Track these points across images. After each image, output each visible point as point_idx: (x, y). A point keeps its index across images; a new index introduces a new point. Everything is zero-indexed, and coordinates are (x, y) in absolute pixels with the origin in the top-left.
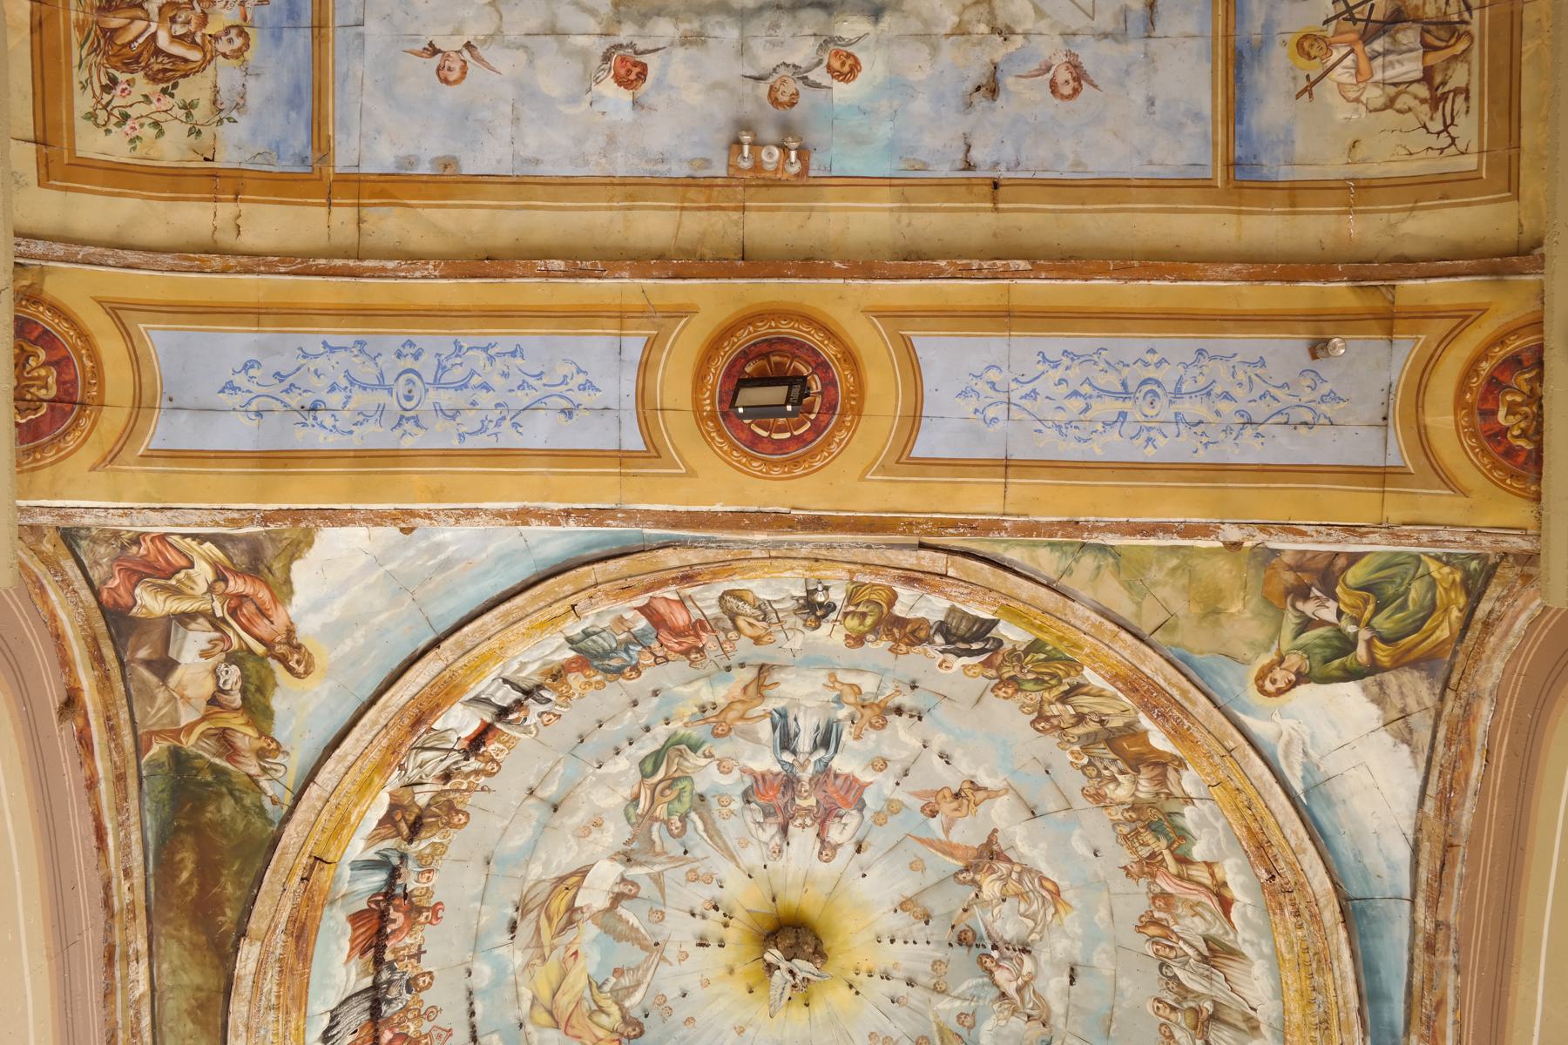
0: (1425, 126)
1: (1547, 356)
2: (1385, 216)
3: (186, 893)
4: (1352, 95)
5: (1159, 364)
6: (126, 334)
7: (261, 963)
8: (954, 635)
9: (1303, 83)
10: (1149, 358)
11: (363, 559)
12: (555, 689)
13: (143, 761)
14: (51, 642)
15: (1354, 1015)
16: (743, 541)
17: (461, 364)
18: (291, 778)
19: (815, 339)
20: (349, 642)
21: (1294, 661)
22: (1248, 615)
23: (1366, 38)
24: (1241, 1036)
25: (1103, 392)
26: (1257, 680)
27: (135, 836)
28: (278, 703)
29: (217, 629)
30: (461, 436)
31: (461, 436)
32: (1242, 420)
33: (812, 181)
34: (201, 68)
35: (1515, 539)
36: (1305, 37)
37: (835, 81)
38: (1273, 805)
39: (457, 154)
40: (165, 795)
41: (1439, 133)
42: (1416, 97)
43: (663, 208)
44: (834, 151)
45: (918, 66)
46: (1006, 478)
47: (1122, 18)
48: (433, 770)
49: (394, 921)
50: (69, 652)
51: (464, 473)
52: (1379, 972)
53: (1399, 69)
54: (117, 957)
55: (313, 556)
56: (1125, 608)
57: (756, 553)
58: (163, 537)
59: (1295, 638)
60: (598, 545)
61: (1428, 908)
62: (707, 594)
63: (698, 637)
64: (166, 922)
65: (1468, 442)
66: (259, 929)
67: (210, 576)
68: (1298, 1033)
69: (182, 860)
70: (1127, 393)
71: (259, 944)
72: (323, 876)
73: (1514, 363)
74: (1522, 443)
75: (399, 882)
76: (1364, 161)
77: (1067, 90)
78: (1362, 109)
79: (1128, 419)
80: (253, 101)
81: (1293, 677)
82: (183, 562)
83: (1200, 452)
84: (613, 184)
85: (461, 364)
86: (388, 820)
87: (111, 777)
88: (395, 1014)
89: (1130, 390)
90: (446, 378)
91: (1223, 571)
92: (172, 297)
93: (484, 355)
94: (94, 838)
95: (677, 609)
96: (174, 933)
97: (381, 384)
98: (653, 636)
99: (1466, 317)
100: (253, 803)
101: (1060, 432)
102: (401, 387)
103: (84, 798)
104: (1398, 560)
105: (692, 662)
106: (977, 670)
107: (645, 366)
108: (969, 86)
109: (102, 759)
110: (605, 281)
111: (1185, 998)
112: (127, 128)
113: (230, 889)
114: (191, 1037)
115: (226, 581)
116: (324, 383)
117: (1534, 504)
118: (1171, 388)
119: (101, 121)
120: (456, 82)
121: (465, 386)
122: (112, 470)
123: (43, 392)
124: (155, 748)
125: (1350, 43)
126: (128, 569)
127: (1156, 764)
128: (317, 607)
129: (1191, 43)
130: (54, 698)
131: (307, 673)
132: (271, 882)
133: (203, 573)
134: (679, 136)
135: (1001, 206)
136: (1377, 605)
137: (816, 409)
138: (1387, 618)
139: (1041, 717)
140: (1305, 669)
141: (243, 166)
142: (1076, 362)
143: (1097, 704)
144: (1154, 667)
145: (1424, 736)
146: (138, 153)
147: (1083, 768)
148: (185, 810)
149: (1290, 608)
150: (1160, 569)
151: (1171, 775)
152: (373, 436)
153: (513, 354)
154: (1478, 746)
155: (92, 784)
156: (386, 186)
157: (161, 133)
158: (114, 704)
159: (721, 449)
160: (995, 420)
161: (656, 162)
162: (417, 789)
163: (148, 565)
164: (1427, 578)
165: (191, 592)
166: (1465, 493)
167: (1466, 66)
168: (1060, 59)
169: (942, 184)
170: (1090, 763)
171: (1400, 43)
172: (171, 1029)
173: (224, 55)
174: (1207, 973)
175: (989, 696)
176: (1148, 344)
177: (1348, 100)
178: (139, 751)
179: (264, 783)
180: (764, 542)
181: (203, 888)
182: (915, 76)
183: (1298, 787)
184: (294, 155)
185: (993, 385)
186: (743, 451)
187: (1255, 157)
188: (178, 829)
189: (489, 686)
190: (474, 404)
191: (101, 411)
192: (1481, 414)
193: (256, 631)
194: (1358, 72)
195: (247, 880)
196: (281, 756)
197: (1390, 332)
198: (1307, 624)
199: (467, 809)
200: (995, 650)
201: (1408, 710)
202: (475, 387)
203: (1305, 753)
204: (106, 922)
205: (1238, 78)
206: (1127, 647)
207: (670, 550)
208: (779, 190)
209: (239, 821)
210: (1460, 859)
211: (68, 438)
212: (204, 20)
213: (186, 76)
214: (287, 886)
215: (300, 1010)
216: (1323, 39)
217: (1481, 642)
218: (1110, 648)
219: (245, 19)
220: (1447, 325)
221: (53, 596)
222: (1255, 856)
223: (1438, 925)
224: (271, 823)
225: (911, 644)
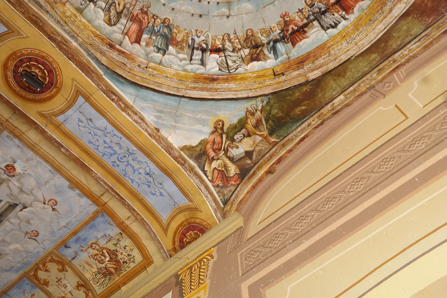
3: (308, 104)
6: (169, 224)
7: (313, 70)
11: (178, 131)
12: (187, 41)
13: (279, 140)
14: (256, 188)
16: (81, 46)
17: (106, 151)
18: (253, 102)
19: (11, 80)
20: (203, 117)
27: (299, 129)
28: (235, 121)
29: (228, 150)
30: (121, 138)
31: (121, 138)
34: (105, 248)
39: (67, 188)
40: (285, 128)
43: (28, 137)
48: (235, 56)
49: (292, 28)
50: (256, 182)
51: (128, 131)
54: (335, 111)
55: (187, 143)
57: (81, 40)
58: (211, 181)
60: (118, 81)
62: (117, 30)
63: (137, 15)
64: (321, 102)
66: (302, 79)
67: (215, 161)
69: (299, 111)
71: (307, 75)
72: (278, 70)
75: (278, 37)
80: (102, 234)
82: (216, 171)
84: (36, 152)
85: (106, 151)
86: (257, 59)
87: (284, 148)
88: (323, 4)
90: (112, 152)
92: (154, 220)
93: (99, 148)
94: (305, 140)
95: (130, 34)
96: (322, 98)
97: (128, 164)
98: (147, 29)
100: (268, 106)
102: (125, 159)
103: (295, 150)
105: (148, 7)
109: (280, 154)
110: (55, 137)
112: (130, 253)
113: (297, 94)
114: (351, 71)
115: (213, 158)
116: (140, 176)
119: (133, 259)
120: (54, 200)
121: (110, 146)
122: (199, 207)
123: (192, 234)
124: (273, 140)
126: (227, 182)
128: (201, 132)
130: (270, 177)
131: (220, 121)
132: (286, 86)
133: (215, 164)
134: (10, 147)
137: (26, 64)
141: (116, 226)
146: (133, 248)
148: (284, 121)
152: (141, 156)
153: (91, 143)
155: (290, 151)
156: (89, 195)
157: (125, 246)
158: (264, 161)
159: (60, 78)
161: (21, 147)
162: (244, 56)
163: (222, 178)
165: (223, 163)
172: (352, 78)
173: (99, 246)
178: (276, 143)
179: (260, 108)
180: (75, 41)
181: (303, 100)
184: (104, 218)
186: (55, 72)
188: (291, 119)
189: (195, 64)
190: (111, 142)
191: (188, 219)
193: (220, 140)
195: (291, 92)
196: (249, 109)
199: (245, 33)
202: (108, 144)
204: (328, 120)
207: (102, 62)
209: (276, 106)
211: (198, 222)
212: (96, 255)
213: (110, 250)
214: (284, 81)
215: (326, 44)
219: (88, 247)
221: (242, 197)
224: (269, 98)
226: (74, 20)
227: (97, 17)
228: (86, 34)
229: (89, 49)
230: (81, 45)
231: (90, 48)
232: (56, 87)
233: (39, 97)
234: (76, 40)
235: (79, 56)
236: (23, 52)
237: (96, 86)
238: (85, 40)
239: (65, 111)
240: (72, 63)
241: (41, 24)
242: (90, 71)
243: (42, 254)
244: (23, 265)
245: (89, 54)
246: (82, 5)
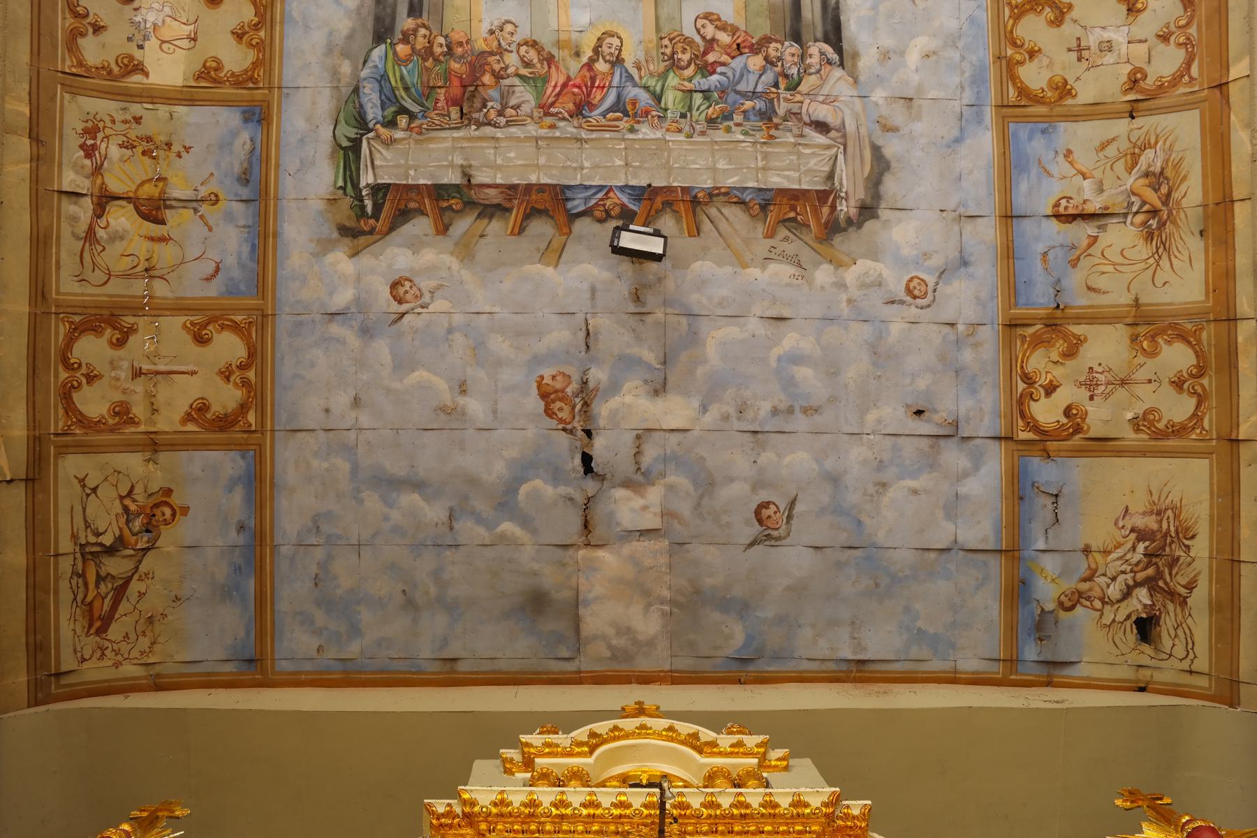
243: (985, 17)
244: (976, 90)
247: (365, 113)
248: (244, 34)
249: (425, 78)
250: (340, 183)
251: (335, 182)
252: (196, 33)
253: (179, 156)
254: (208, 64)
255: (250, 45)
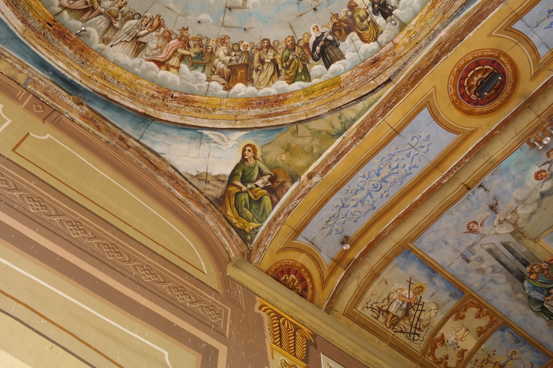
0: (376, 303)
1: (303, 299)
2: (362, 278)
4: (398, 291)
5: (382, 195)
8: (329, 45)
9: (412, 282)
10: (386, 194)
15: (105, 93)
16: (446, 26)
19: (486, 108)
21: (252, 162)
22: (278, 159)
23: (409, 304)
24: (101, 33)
25: (390, 174)
26: (254, 146)
32: (345, 205)
33: (523, 141)
35: (258, 259)
36: (423, 290)
37: (539, 169)
38: (206, 120)
41: (372, 305)
42: (385, 306)
44: (524, 154)
45: (518, 194)
46: (394, 130)
47: (473, 252)
52: (117, 112)
53: (395, 306)
56: (313, 125)
57: (438, 26)
59: (259, 167)
61: (137, 147)
65: (291, 262)
68: (103, 64)
70: (383, 181)
73: (305, 289)
74: (284, 278)
76: (380, 283)
77: (471, 225)
78: (393, 291)
79: (376, 176)
81: (246, 157)
83: (348, 188)
89: (383, 182)
91: (300, 163)
99: (324, 283)
101: (391, 155)
104: (264, 217)
106: (306, 39)
107: (534, 49)
108: (499, 202)
111: (123, 16)
117: (266, 271)
118: (372, 193)
125: (411, 299)
127: (229, 78)
129: (450, 263)
135: (462, 185)
136: (252, 199)
137: (467, 91)
138: (245, 199)
139: (269, 46)
140: (246, 163)
142: (405, 174)
143: (266, 75)
144: (286, 119)
145: (195, 182)
147: (239, 45)
149: (270, 173)
150: (316, 145)
151: (222, 81)
154: (186, 200)
159: (486, 52)
160: (413, 139)
164: (251, 220)
166: (278, 252)
167: (383, 322)
168: (480, 229)
169: (484, 175)
170: (240, 50)
171: (400, 310)
174: (131, 34)
175: (291, 34)
176: (390, 197)
177: (398, 289)
182: (517, 191)
183: (205, 132)
185: (422, 147)
186: (479, 57)
187: (406, 257)
192: (297, 271)
194: (403, 296)
197: (335, 261)
198: (261, 174)
200: (312, 54)
201: (208, 184)
203: (216, 142)
205: (429, 268)
206: (300, 116)
208: (532, 130)
210: (148, 169)
216: (418, 294)
217: (224, 224)
218: (304, 110)
220: (325, 276)
222: (184, 97)
223: (129, 147)
225: (335, 24)
226: (414, 33)
227: (410, 6)
228: (431, 19)
229: (450, 15)
230: (444, 25)
231: (449, 14)
232: (498, 58)
233: (510, 78)
234: (439, 31)
235: (459, 28)
236: (452, 93)
237: (501, 6)
238: (439, 20)
239: (533, 45)
240: (467, 37)
241: (419, 72)
242: (479, 14)
245: (456, 15)
246: (396, 24)
247: (538, 299)
248: (480, 315)
249: (548, 276)
250: (548, 319)
251: (546, 320)
252: (466, 328)
253: (494, 354)
254: (478, 331)
255: (484, 316)
